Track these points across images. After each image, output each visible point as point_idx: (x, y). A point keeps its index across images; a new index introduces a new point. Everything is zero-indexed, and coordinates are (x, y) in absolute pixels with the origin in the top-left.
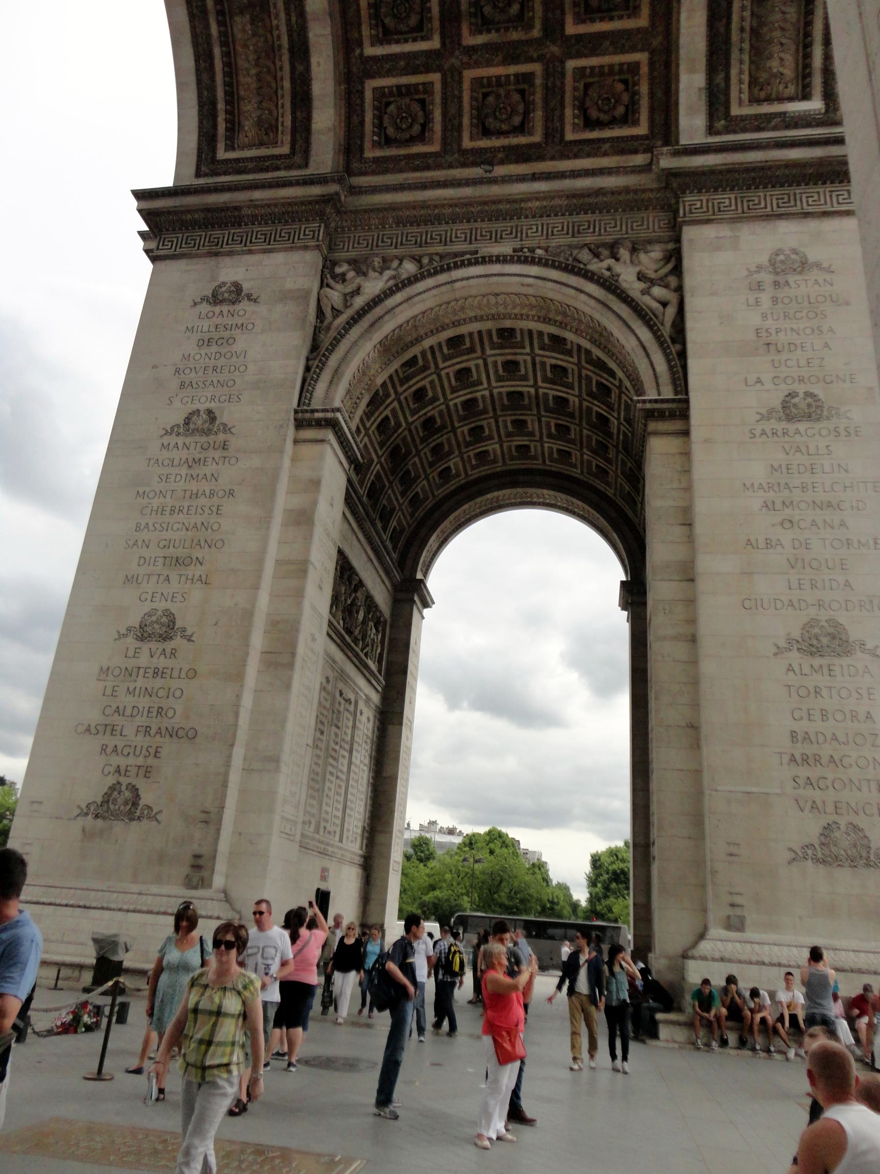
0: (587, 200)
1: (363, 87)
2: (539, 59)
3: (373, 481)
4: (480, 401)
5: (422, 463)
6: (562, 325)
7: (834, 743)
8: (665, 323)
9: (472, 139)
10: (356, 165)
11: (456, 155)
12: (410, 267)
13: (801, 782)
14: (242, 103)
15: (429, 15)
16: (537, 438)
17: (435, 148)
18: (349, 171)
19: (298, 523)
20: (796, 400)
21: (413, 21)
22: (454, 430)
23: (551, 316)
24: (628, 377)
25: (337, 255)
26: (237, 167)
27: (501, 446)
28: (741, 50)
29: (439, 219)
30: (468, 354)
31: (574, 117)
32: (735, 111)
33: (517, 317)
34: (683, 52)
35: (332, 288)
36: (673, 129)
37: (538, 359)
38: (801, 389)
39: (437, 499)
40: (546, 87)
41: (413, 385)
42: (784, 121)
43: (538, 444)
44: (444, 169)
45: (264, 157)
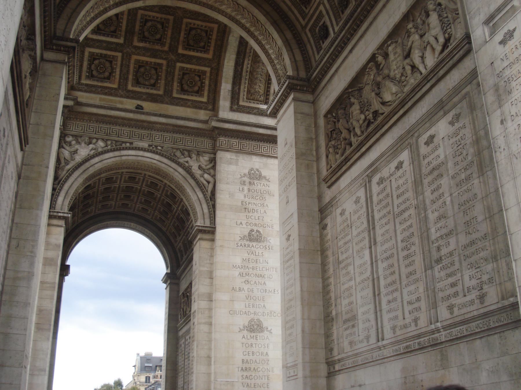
1: (84, 50)
7: (256, 363)
12: (101, 144)
13: (244, 377)
17: (115, 86)
19: (51, 265)
20: (253, 233)
21: (112, 28)
24: (190, 206)
27: (116, 203)
28: (246, 79)
29: (116, 124)
32: (241, 103)
34: (224, 74)
35: (64, 148)
37: (146, 179)
38: (255, 229)
40: (167, 71)
42: (258, 111)
43: (134, 204)
44: (118, 97)
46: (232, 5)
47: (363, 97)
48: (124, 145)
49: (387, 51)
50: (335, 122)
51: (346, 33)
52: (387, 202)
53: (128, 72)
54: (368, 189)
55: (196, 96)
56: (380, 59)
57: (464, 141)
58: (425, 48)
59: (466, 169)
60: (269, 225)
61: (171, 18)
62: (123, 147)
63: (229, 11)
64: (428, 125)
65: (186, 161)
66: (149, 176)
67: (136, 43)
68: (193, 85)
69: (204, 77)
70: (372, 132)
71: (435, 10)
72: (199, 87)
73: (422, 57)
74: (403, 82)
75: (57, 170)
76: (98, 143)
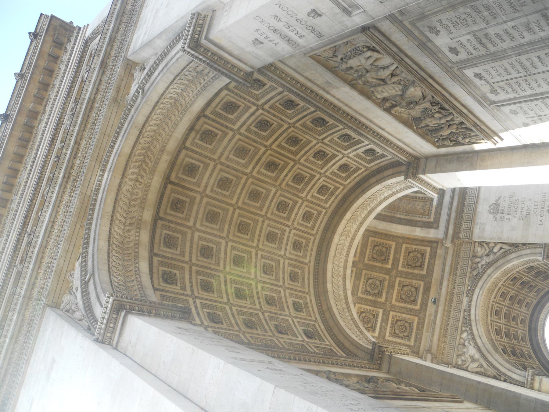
0: (453, 269)
2: (396, 278)
9: (416, 305)
12: (465, 335)
16: (520, 313)
17: (416, 319)
21: (371, 317)
22: (515, 345)
24: (523, 265)
27: (520, 329)
28: (412, 216)
31: (418, 269)
32: (432, 220)
35: (468, 366)
37: (498, 301)
40: (404, 278)
43: (522, 314)
46: (351, 224)
47: (420, 116)
48: (466, 317)
49: (381, 100)
50: (443, 139)
51: (369, 134)
52: (514, 84)
53: (405, 308)
54: (502, 104)
55: (425, 256)
56: (388, 105)
57: (452, 18)
58: (376, 66)
59: (479, 12)
60: (543, 197)
61: (364, 272)
62: (468, 317)
63: (355, 227)
64: (440, 55)
65: (481, 266)
66: (495, 298)
67: (383, 300)
70: (449, 105)
71: (346, 63)
73: (384, 68)
74: (405, 82)
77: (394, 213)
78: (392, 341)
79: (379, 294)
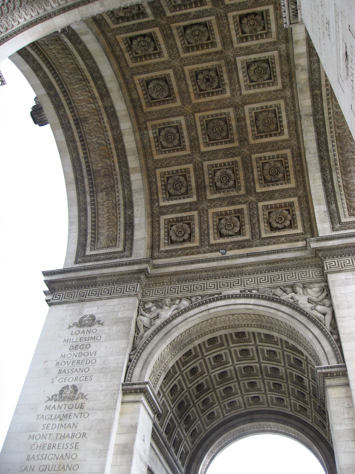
0: (277, 265)
2: (245, 203)
3: (168, 423)
4: (229, 372)
5: (197, 411)
6: (270, 329)
8: (326, 324)
10: (156, 254)
11: (207, 247)
12: (185, 303)
14: (100, 229)
15: (190, 187)
16: (263, 392)
17: (196, 244)
18: (152, 257)
21: (183, 190)
22: (215, 390)
23: (264, 324)
24: (310, 355)
25: (146, 299)
26: (97, 258)
27: (243, 398)
28: (341, 194)
29: (200, 278)
30: (220, 347)
32: (343, 220)
33: (245, 326)
36: (315, 229)
37: (259, 348)
39: (207, 432)
41: (190, 366)
43: (264, 395)
44: (201, 253)
45: (109, 253)
53: (208, 228)
61: (238, 159)
68: (283, 221)
69: (293, 208)
72: (290, 221)
75: (135, 339)
76: (181, 303)
77: (336, 169)
78: (159, 225)
79: (216, 190)
